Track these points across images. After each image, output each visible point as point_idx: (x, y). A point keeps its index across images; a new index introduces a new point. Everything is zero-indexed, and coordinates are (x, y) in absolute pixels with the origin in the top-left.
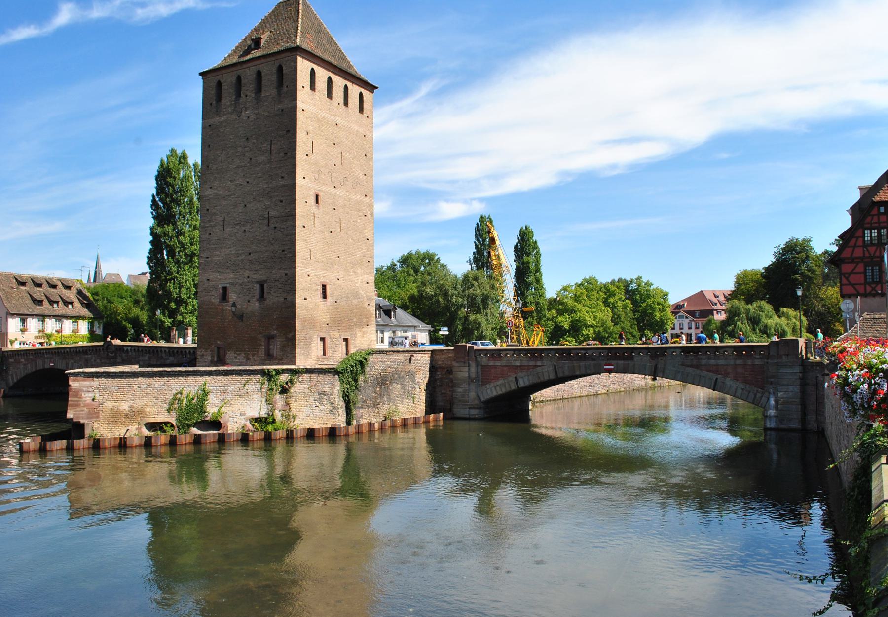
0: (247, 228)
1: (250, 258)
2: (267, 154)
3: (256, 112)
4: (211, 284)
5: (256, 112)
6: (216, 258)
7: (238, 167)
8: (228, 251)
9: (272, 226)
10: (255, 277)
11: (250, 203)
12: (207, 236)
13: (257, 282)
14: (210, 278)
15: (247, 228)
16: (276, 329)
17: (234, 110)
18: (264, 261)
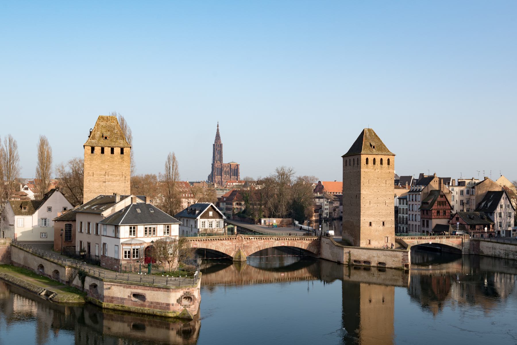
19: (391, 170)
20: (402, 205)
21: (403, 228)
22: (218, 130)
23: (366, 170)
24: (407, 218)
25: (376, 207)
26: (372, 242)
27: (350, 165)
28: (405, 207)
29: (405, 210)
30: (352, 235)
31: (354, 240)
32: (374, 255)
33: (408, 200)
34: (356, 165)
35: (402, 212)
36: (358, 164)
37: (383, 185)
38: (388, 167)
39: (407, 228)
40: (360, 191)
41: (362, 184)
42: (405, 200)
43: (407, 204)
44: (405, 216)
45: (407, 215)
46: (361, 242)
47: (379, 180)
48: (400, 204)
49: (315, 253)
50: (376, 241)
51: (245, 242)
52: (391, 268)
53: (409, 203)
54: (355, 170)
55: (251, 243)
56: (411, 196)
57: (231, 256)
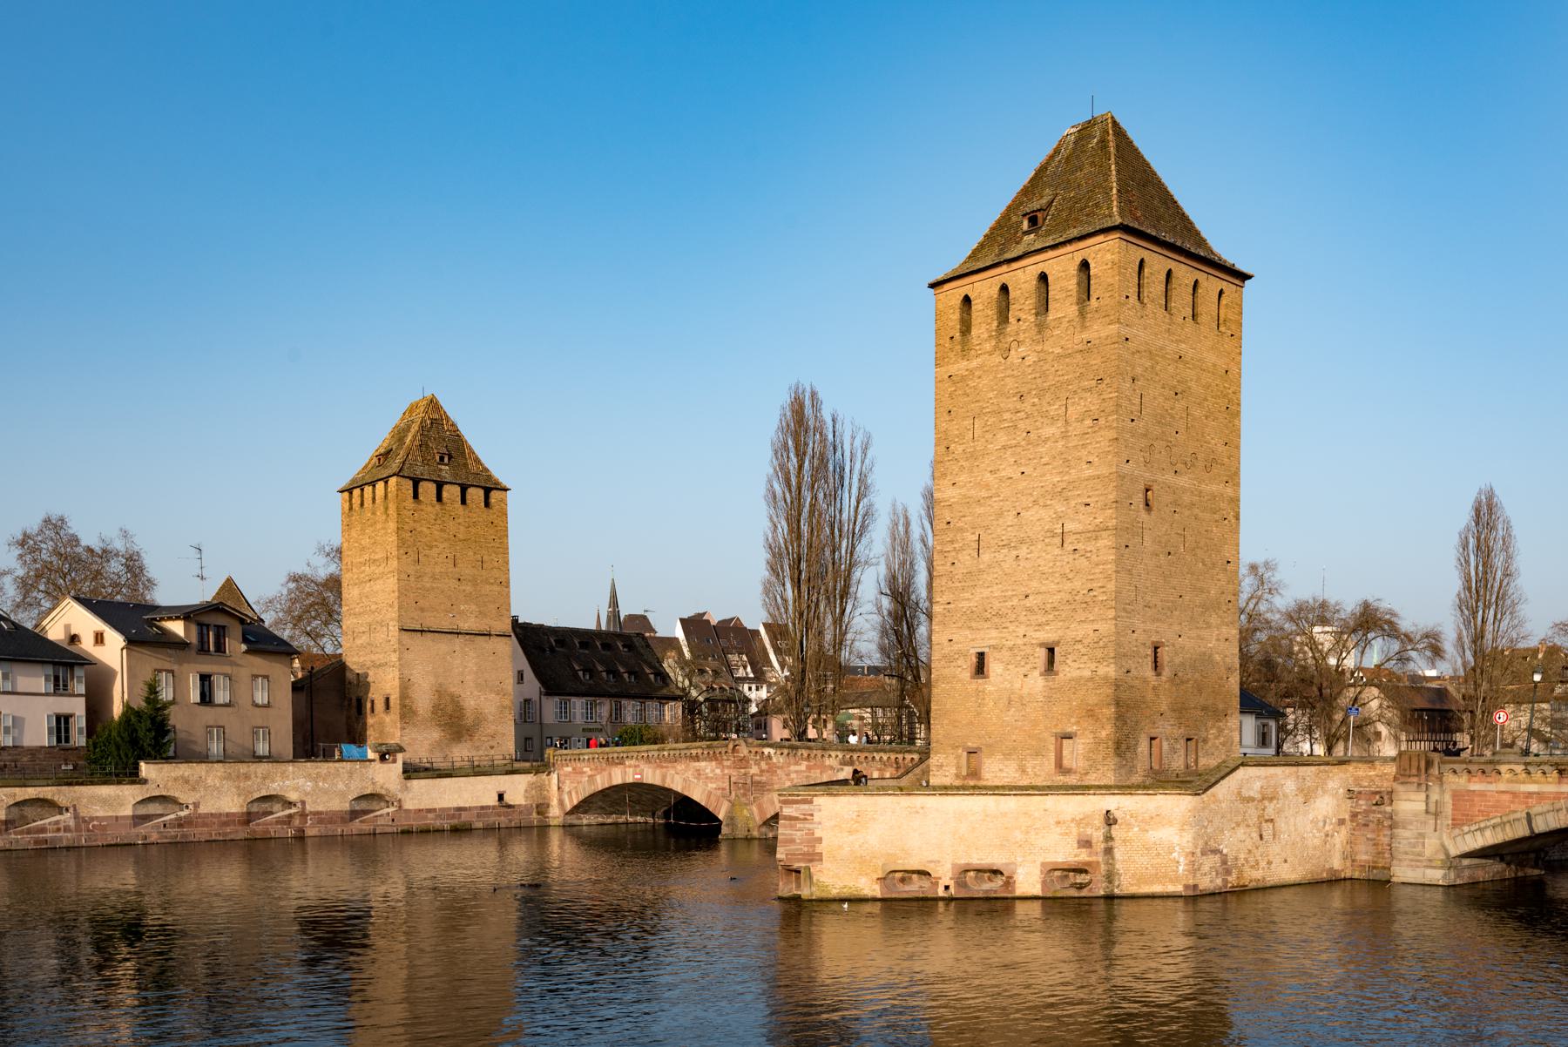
0: (1023, 551)
1: (1028, 603)
6: (965, 604)
7: (1004, 448)
8: (986, 593)
10: (1038, 635)
13: (1041, 645)
14: (954, 637)
17: (996, 347)
37: (1049, 431)
47: (1027, 406)
50: (1007, 756)
51: (754, 770)
55: (772, 770)
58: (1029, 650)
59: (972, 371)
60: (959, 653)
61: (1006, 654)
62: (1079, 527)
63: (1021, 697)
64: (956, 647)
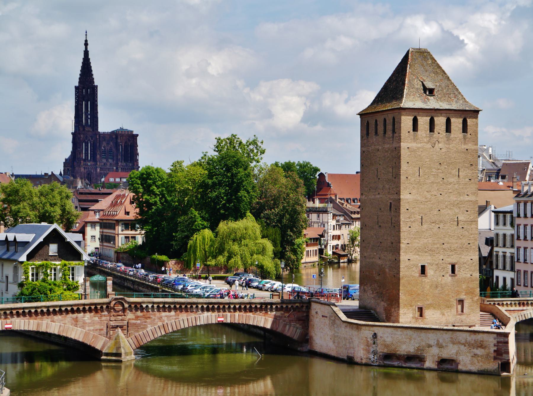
0: (441, 226)
2: (457, 178)
3: (447, 146)
4: (411, 263)
5: (447, 146)
7: (432, 182)
8: (425, 241)
9: (460, 226)
10: (448, 259)
11: (443, 209)
12: (408, 228)
13: (449, 264)
15: (441, 226)
16: (465, 295)
18: (455, 250)
19: (470, 146)
20: (501, 226)
21: (505, 279)
22: (86, 53)
23: (413, 145)
24: (512, 257)
25: (435, 229)
26: (427, 313)
27: (376, 133)
28: (509, 231)
29: (508, 239)
30: (380, 295)
31: (385, 309)
32: (432, 342)
33: (515, 215)
34: (389, 133)
35: (501, 243)
36: (394, 131)
37: (451, 180)
38: (465, 138)
39: (512, 280)
40: (398, 193)
41: (403, 178)
42: (508, 216)
43: (512, 225)
44: (509, 251)
45: (514, 250)
46: (402, 311)
47: (442, 167)
48: (497, 224)
49: (296, 337)
52: (469, 373)
53: (517, 221)
54: (387, 146)
56: (522, 205)
57: (98, 347)
58: (444, 265)
59: (418, 148)
60: (414, 265)
61: (434, 267)
62: (465, 220)
63: (441, 284)
64: (411, 263)
